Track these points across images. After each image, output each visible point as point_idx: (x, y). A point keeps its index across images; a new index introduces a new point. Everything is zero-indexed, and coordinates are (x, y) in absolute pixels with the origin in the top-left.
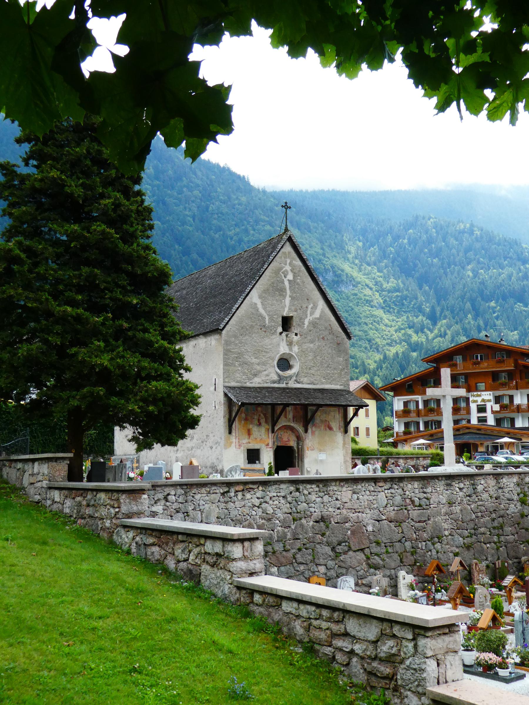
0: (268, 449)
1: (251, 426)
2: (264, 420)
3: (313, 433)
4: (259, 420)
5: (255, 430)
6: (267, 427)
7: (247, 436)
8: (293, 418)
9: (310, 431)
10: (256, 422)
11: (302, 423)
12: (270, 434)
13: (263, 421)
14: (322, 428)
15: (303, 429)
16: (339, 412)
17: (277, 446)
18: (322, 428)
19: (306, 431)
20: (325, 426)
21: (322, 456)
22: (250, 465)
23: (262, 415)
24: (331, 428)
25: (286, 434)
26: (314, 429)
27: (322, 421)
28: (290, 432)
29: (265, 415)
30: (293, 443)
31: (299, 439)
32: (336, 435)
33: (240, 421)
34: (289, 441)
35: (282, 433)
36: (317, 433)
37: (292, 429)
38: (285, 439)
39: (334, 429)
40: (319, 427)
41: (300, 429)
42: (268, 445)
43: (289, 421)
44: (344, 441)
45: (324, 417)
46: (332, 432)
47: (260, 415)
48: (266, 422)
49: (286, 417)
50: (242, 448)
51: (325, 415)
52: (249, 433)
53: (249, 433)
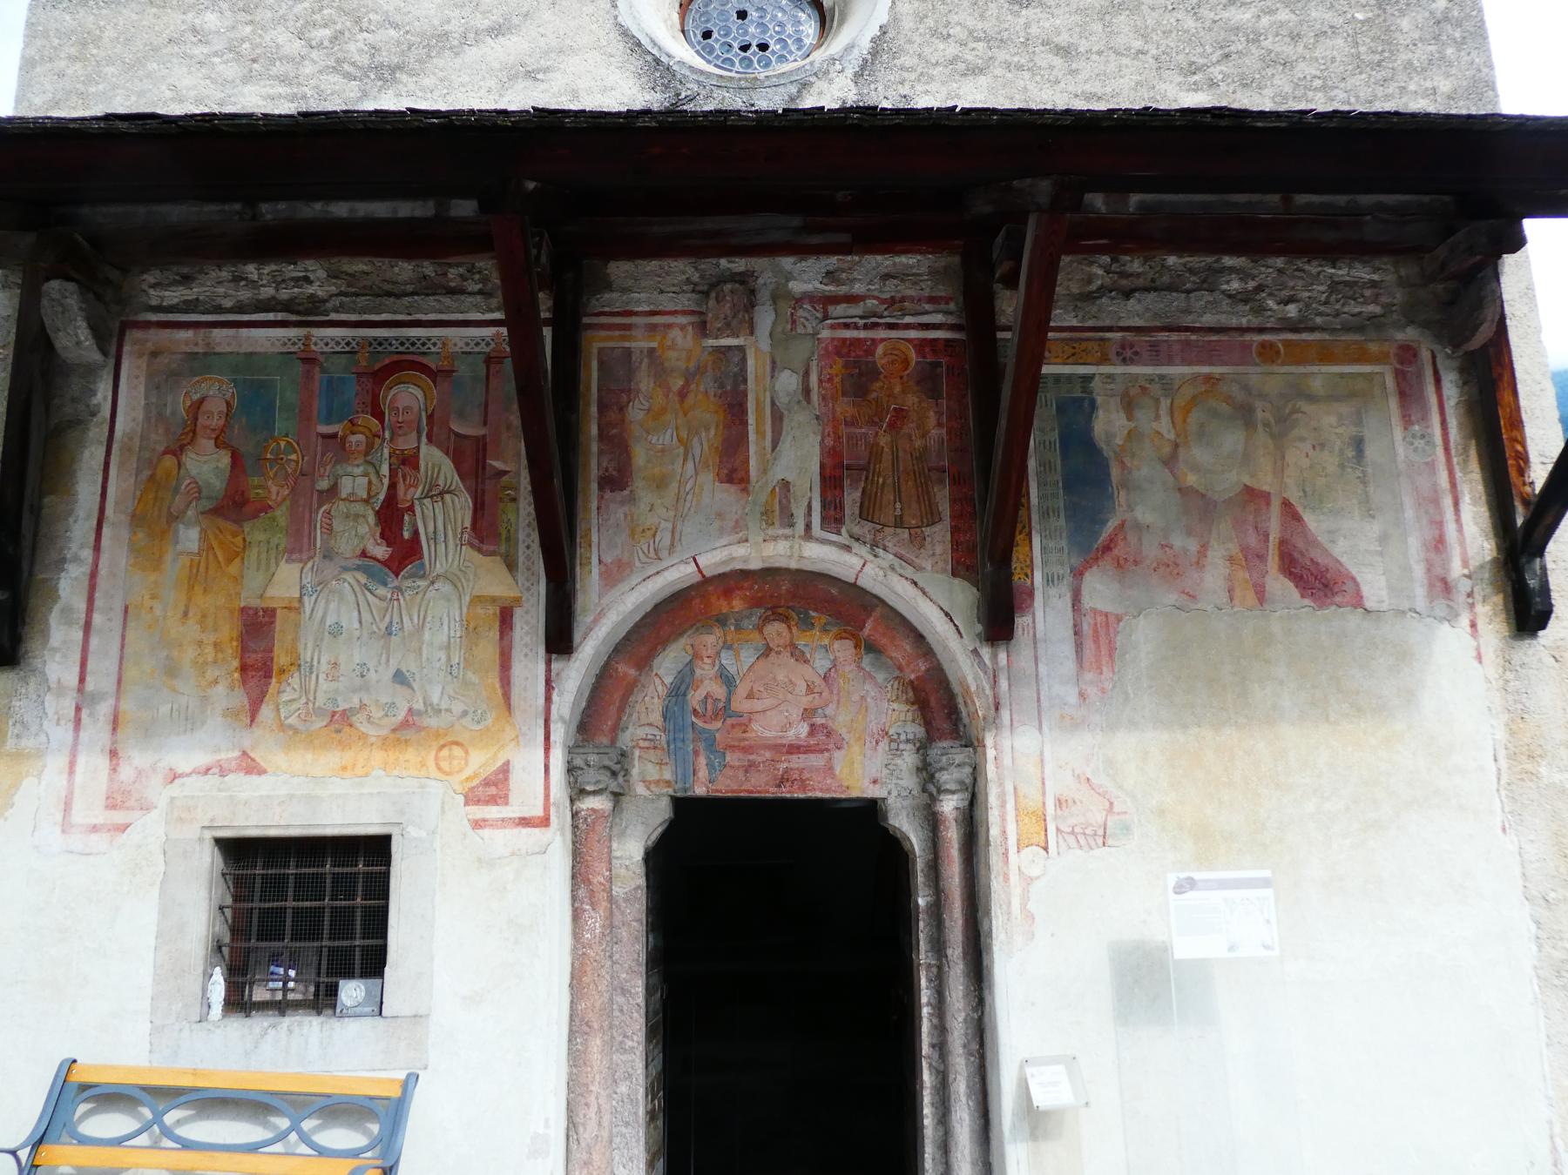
0: (502, 840)
1: (286, 580)
2: (461, 507)
3: (1095, 641)
4: (391, 516)
5: (336, 619)
6: (493, 581)
7: (226, 693)
8: (831, 481)
9: (1046, 616)
10: (359, 533)
11: (940, 536)
12: (529, 665)
13: (442, 520)
14: (1214, 577)
15: (964, 596)
16: (1408, 395)
17: (684, 806)
18: (1214, 577)
19: (999, 619)
20: (1251, 558)
21: (1215, 925)
22: (241, 1029)
23: (433, 459)
24: (1320, 582)
25: (784, 669)
26: (1100, 590)
27: (1199, 507)
28: (827, 652)
29: (473, 461)
30: (867, 763)
31: (942, 716)
32: (1404, 656)
33: (153, 520)
34: (823, 738)
35: (742, 660)
36: (1143, 638)
37: (848, 610)
38: (777, 718)
39: (1374, 585)
40: (1171, 568)
41: (934, 603)
42: (494, 788)
43: (779, 511)
44: (1518, 716)
45: (1221, 459)
46: (1338, 620)
47: (408, 461)
48: (485, 531)
49: (734, 474)
50: (150, 829)
51: (1232, 440)
52: (259, 654)
53: (259, 654)
